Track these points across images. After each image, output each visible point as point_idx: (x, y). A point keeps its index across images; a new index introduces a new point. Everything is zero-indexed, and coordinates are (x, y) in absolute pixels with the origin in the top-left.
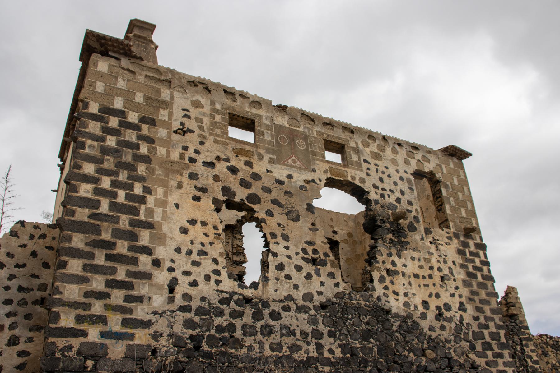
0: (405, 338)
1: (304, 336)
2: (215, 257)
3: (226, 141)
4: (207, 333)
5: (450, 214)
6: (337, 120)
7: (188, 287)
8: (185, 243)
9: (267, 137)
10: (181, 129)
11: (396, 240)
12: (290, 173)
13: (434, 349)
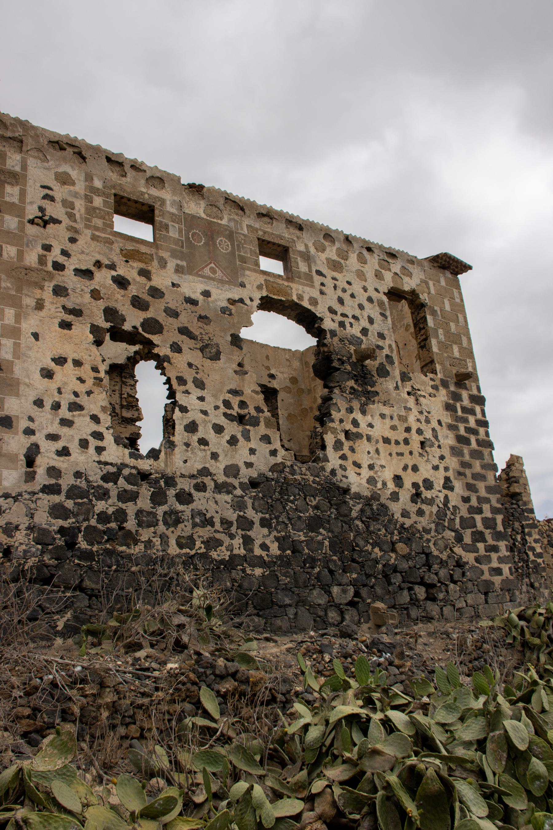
0: (368, 527)
1: (226, 526)
2: (95, 413)
3: (111, 237)
4: (85, 524)
5: (437, 354)
6: (279, 209)
7: (56, 457)
8: (49, 392)
9: (173, 233)
10: (40, 218)
11: (360, 389)
12: (207, 288)
13: (408, 541)
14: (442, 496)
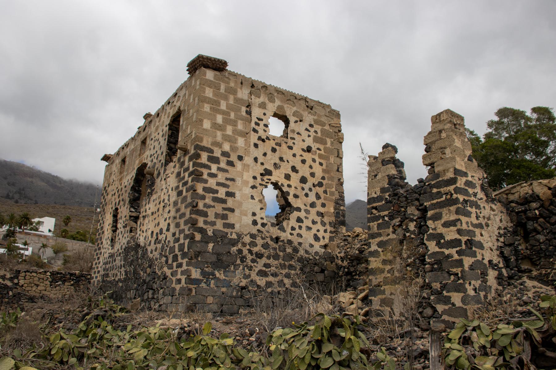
14: (164, 236)
